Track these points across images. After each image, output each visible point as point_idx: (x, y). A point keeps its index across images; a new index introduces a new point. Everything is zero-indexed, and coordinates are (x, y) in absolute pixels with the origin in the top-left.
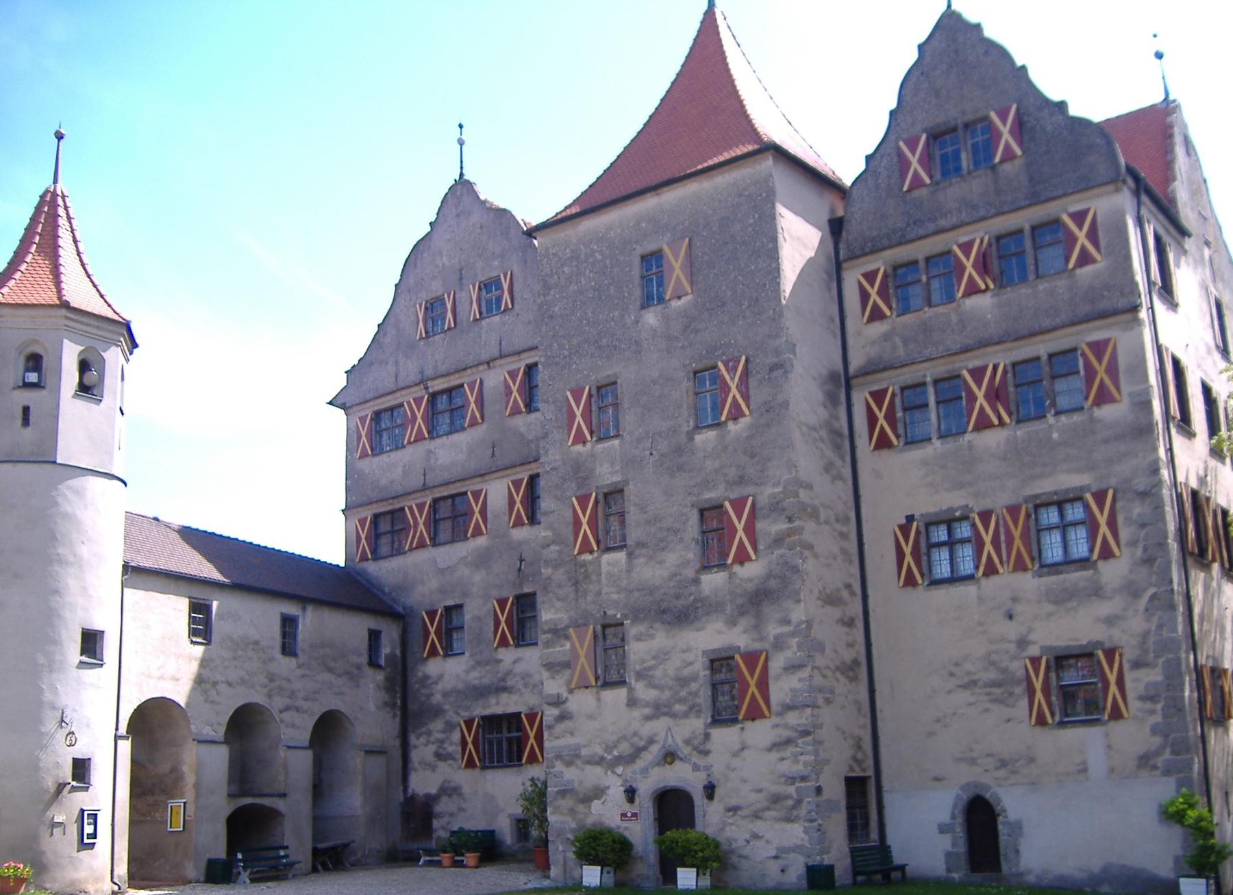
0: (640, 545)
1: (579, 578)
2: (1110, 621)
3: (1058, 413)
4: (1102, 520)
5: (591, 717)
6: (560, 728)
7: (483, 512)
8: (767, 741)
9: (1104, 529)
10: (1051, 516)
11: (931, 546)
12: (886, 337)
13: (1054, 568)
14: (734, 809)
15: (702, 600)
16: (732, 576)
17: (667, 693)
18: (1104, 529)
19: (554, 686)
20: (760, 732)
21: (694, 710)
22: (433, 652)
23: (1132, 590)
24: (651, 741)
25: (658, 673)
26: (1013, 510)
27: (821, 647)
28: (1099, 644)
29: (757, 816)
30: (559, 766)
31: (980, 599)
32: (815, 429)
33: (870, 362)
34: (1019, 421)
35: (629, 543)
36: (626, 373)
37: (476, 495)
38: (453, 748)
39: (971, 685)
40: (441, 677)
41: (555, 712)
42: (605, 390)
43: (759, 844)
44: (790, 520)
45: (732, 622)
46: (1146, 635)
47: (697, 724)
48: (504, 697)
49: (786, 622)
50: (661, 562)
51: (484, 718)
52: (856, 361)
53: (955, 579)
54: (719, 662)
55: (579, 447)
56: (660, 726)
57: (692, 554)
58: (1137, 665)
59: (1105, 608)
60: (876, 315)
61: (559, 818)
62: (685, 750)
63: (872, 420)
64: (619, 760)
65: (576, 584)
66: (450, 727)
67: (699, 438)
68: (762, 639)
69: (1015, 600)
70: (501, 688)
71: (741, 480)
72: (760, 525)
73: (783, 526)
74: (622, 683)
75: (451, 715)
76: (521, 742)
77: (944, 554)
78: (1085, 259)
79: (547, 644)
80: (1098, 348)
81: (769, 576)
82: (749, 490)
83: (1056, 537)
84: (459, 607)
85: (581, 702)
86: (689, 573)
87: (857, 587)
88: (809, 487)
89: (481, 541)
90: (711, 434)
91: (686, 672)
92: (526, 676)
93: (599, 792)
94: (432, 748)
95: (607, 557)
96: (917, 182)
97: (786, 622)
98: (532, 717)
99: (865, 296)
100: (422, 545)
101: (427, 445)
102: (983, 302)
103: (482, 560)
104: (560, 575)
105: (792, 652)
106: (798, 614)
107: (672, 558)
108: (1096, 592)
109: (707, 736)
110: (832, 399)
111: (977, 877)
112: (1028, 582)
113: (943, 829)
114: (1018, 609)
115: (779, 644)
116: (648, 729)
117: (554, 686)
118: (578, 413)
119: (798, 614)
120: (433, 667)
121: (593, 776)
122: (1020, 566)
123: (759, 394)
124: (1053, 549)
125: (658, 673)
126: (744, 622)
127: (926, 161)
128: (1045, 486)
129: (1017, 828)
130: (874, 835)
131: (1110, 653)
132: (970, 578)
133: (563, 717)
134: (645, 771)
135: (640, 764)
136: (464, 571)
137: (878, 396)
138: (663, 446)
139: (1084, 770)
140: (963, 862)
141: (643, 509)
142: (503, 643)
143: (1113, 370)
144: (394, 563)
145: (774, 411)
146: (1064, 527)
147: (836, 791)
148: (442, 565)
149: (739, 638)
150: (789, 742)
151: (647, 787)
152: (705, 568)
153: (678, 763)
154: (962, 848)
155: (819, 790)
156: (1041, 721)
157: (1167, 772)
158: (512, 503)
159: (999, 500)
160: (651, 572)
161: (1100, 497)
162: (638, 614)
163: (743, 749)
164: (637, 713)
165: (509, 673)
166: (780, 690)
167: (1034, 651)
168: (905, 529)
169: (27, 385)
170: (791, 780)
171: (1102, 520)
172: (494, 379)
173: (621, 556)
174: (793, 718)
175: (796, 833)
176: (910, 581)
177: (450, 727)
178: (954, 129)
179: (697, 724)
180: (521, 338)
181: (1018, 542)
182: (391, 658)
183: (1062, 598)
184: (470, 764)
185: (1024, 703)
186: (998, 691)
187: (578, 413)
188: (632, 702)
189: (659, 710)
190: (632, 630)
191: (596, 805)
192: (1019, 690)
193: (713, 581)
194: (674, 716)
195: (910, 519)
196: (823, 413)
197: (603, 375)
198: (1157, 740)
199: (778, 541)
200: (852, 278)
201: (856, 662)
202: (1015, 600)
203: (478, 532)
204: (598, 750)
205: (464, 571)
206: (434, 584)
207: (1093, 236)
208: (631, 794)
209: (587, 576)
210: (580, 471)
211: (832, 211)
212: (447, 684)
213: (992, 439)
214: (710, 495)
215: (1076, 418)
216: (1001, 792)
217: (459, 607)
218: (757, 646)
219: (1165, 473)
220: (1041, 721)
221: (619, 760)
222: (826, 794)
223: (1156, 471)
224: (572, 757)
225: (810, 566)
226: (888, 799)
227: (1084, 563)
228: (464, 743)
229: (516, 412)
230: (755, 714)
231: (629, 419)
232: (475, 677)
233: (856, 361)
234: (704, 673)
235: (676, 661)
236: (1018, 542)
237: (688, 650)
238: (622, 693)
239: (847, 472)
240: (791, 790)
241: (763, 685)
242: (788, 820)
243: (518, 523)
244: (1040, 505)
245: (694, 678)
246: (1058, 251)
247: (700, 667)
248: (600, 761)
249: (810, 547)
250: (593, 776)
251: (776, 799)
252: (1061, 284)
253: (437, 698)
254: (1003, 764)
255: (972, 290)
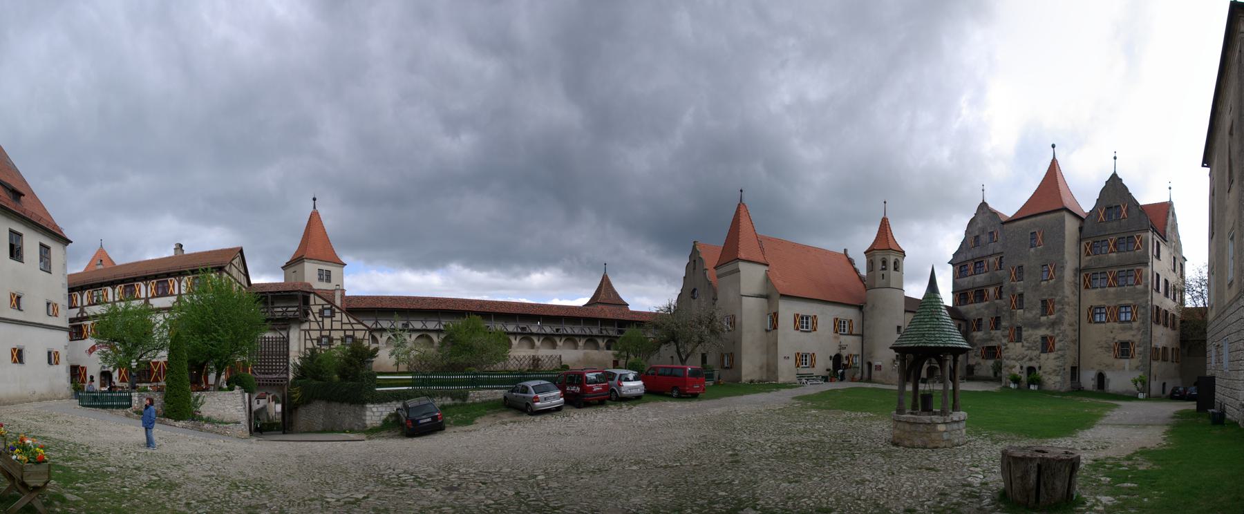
0: (1027, 308)
1: (1012, 315)
2: (1133, 336)
3: (1128, 285)
4: (1134, 312)
5: (1013, 349)
6: (1005, 351)
7: (988, 295)
8: (1053, 357)
9: (1134, 314)
10: (1123, 309)
11: (1096, 314)
12: (1091, 260)
13: (1123, 322)
14: (1045, 372)
15: (1040, 323)
16: (1048, 318)
17: (1031, 345)
18: (1134, 314)
19: (1004, 341)
20: (1052, 355)
21: (1037, 349)
22: (974, 330)
23: (1139, 329)
24: (1027, 356)
25: (1029, 340)
26: (1115, 307)
27: (1067, 336)
28: (1129, 340)
29: (1050, 374)
30: (1005, 360)
31: (1106, 328)
32: (1070, 283)
33: (1086, 266)
34: (1119, 286)
35: (1024, 307)
36: (1026, 265)
37: (986, 290)
38: (979, 353)
39: (1102, 347)
40: (976, 336)
41: (1004, 347)
42: (1021, 267)
43: (1050, 381)
44: (1063, 305)
45: (1047, 329)
46: (1141, 339)
47: (1038, 352)
48: (992, 342)
49: (1060, 330)
50: (1031, 313)
51: (987, 347)
52: (1082, 266)
53: (1101, 322)
54: (1044, 338)
55: (1013, 282)
56: (1029, 352)
57: (1039, 312)
58: (1138, 346)
59: (1133, 333)
60: (1088, 255)
61: (1004, 372)
62: (1035, 358)
63: (1085, 281)
64: (1019, 360)
65: (1011, 317)
66: (978, 348)
67: (1042, 283)
68: (1054, 333)
69: (1113, 328)
70: (991, 340)
71: (1052, 295)
72: (1055, 306)
73: (1061, 307)
74: (1021, 341)
75: (979, 346)
76: (996, 353)
77: (1098, 316)
78: (1138, 248)
79: (1003, 331)
80: (1138, 270)
81: (1056, 319)
82: (1053, 297)
83: (1124, 315)
84: (981, 319)
85: (1011, 345)
86: (1038, 316)
87: (1078, 322)
88: (1068, 297)
89: (987, 303)
90: (1045, 282)
91: (1036, 340)
92: (997, 337)
93: (1014, 367)
94: (974, 354)
95: (1018, 311)
96: (1101, 221)
97: (1060, 330)
98: (998, 347)
99: (1086, 249)
100: (972, 303)
101: (974, 276)
102: (1114, 255)
103: (987, 307)
104: (1007, 314)
105: (1061, 337)
106: (1062, 328)
107: (1034, 312)
108: (1131, 329)
109: (1040, 355)
110: (1075, 275)
111: (1099, 391)
112: (1117, 325)
113: (1093, 379)
114: (1114, 331)
115: (1058, 335)
116: (1026, 352)
117: (1004, 341)
118: (1013, 273)
119: (1062, 328)
120: (975, 334)
121: (1013, 363)
122: (1115, 321)
123: (1057, 274)
124: (1123, 318)
125: (1029, 340)
126: (1050, 329)
127: (1105, 214)
128: (1123, 302)
129: (1109, 380)
130: (1077, 380)
131: (1132, 343)
132: (1104, 322)
133: (1007, 348)
134: (1025, 362)
135: (1024, 360)
136: (983, 310)
137: (1087, 275)
138: (1033, 284)
139: (1124, 368)
140: (1096, 388)
141: (1028, 299)
142: (992, 329)
143: (1141, 277)
144: (965, 307)
145: (1061, 278)
146: (1126, 312)
147: (1068, 369)
148: (977, 308)
149: (1048, 333)
150: (1058, 358)
151: (1025, 366)
152: (1042, 315)
153: (1033, 362)
154: (1096, 384)
155: (1064, 369)
156: (1116, 357)
157: (1141, 370)
158: (995, 293)
159: (1112, 304)
160: (1028, 315)
161: (1134, 307)
162: (1025, 325)
163: (1048, 359)
164: (1024, 349)
165: (993, 336)
166: (1057, 346)
167: (1116, 341)
168: (1090, 309)
169: (883, 269)
170: (1058, 366)
171: (1134, 312)
172: (992, 260)
173: (1022, 311)
174: (1059, 352)
175: (1059, 378)
176: (1090, 322)
177: (978, 348)
178: (1111, 207)
179: (1038, 352)
180: (998, 249)
181: (1115, 315)
182: (963, 331)
183: (1124, 329)
184: (983, 358)
185: (1113, 353)
186: (1107, 350)
187: (1013, 273)
188: (1023, 346)
189: (1029, 348)
190: (1024, 329)
191: (1013, 369)
192: (1112, 349)
193: (1043, 319)
194: (1032, 350)
195: (1091, 306)
196: (1073, 279)
197: (1019, 264)
198: (1140, 364)
199: (1059, 310)
200: (1083, 244)
201: (1076, 340)
202: (1113, 328)
203: (986, 300)
204: (1014, 357)
205: (983, 310)
206: (975, 312)
207: (1141, 242)
208: (1021, 367)
209: (1013, 315)
210: (1013, 289)
211: (1080, 224)
212: (978, 338)
213: (1112, 289)
214: (1044, 298)
215: (1132, 287)
216: (1106, 372)
217: (981, 319)
218: (1053, 335)
219: (1150, 303)
220: (1116, 357)
221: (1019, 360)
222: (1066, 370)
223: (1147, 302)
224: (1008, 358)
225: (1066, 317)
226: (1081, 372)
227: (1129, 322)
228: (982, 352)
229: (997, 270)
230: (1051, 351)
231: (1025, 276)
232: (984, 337)
233: (1082, 266)
234: (1040, 340)
235: (1034, 337)
236: (1115, 315)
237: (1036, 335)
238: (1020, 344)
239: (1078, 293)
240: (1058, 369)
241: (1053, 344)
242: (1057, 375)
243: (997, 299)
244: (1121, 306)
245: (1037, 341)
246: (1133, 244)
247: (1039, 339)
248: (1014, 359)
249: (1067, 312)
250: (1013, 363)
251: (1055, 371)
252: (1132, 253)
253: (975, 341)
254: (1107, 366)
255: (1112, 252)
